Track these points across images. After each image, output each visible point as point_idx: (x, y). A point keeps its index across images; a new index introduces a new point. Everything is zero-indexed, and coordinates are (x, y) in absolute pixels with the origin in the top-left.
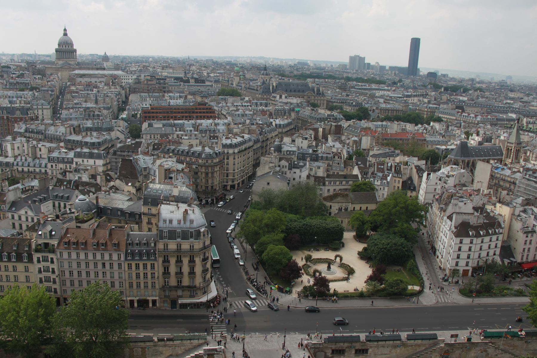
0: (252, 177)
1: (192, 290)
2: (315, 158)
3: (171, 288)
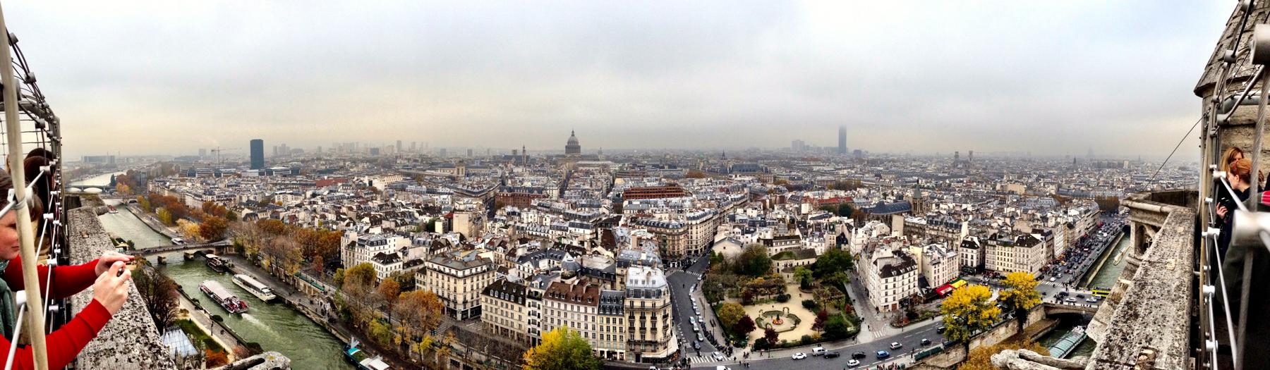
0: (712, 244)
1: (654, 344)
2: (763, 224)
3: (638, 343)
